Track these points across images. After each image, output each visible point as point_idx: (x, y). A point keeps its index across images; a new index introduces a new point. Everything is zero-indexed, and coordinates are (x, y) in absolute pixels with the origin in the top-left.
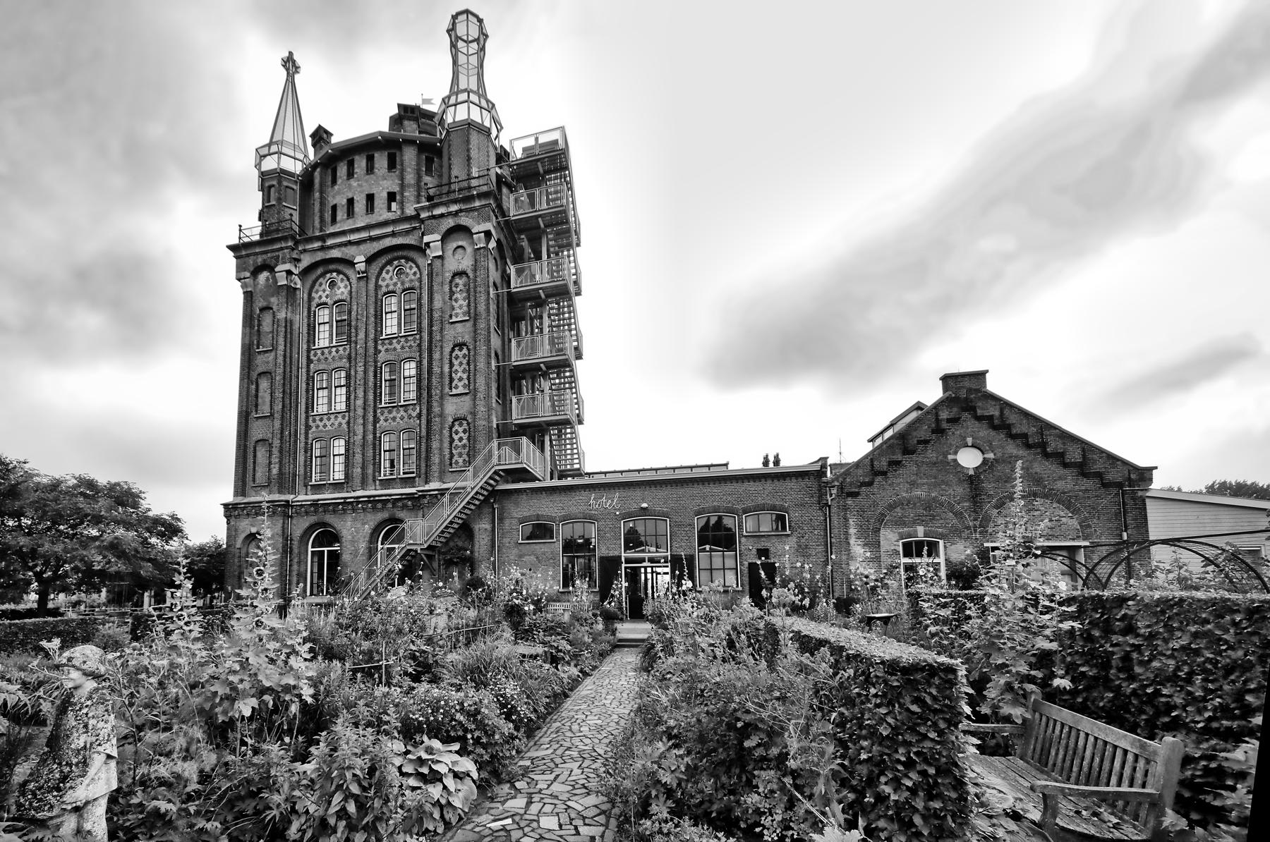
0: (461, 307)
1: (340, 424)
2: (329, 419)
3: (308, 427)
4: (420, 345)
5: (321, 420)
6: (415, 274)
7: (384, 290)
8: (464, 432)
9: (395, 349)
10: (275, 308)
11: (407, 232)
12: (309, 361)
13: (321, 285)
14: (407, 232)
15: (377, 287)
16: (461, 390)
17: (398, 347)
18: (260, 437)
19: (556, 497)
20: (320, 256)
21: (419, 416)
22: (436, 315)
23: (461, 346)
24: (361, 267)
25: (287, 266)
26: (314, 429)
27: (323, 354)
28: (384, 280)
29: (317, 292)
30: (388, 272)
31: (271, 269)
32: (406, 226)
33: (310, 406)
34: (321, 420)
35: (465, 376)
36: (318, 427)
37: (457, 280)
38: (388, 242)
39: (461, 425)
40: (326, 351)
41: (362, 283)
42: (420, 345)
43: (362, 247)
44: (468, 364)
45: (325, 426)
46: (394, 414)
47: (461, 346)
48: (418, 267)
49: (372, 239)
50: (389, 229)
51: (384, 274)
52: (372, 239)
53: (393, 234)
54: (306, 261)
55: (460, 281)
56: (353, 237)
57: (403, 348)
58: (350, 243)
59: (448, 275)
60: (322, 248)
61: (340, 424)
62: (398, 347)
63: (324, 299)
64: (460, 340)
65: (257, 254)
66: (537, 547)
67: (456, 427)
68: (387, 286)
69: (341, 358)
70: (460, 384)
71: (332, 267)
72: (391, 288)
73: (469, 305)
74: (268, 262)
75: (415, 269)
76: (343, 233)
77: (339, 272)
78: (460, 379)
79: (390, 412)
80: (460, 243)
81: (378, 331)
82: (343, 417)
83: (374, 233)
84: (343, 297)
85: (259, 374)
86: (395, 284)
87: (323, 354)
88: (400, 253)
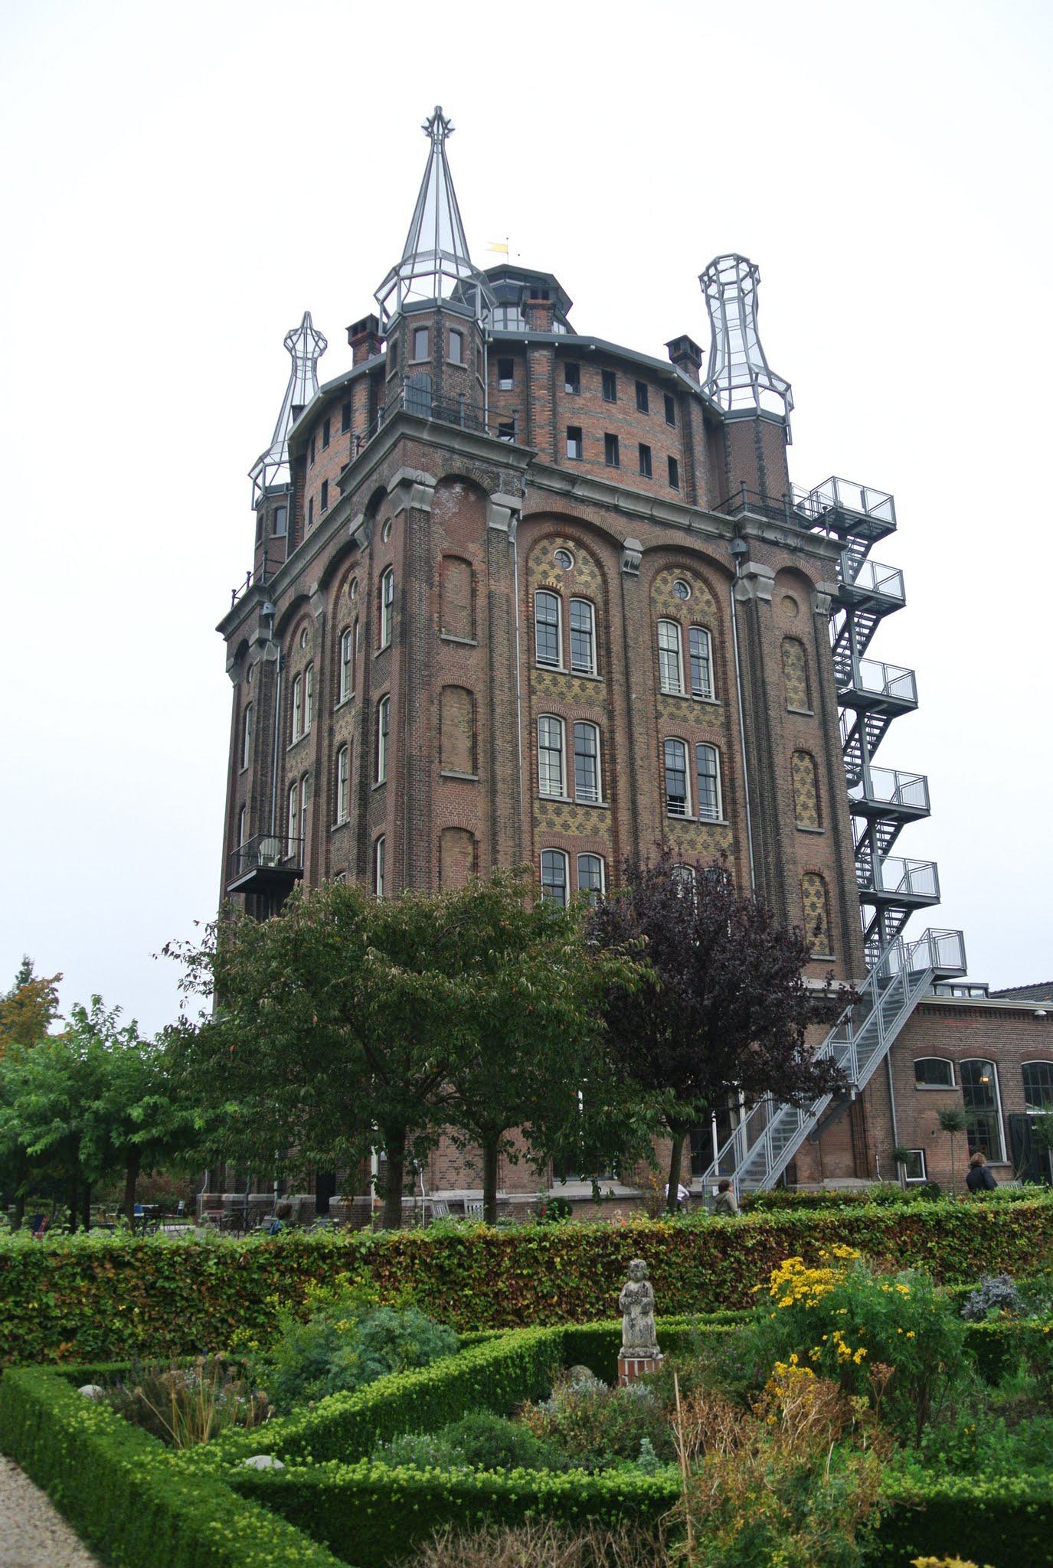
0: (795, 690)
1: (596, 830)
2: (574, 815)
3: (534, 822)
4: (727, 725)
5: (558, 813)
6: (708, 602)
7: (660, 609)
8: (818, 892)
9: (685, 719)
10: (478, 566)
11: (708, 537)
12: (531, 691)
13: (545, 551)
14: (708, 537)
15: (652, 601)
16: (805, 824)
17: (691, 717)
18: (454, 821)
19: (951, 1022)
20: (558, 506)
21: (736, 845)
22: (772, 693)
23: (802, 752)
24: (634, 556)
25: (516, 502)
26: (543, 827)
27: (555, 683)
28: (659, 591)
29: (538, 562)
30: (665, 581)
31: (477, 491)
32: (711, 528)
33: (534, 778)
34: (558, 813)
35: (811, 803)
36: (551, 824)
37: (787, 646)
38: (679, 538)
39: (811, 882)
40: (562, 680)
41: (629, 584)
42: (727, 725)
43: (637, 525)
44: (816, 783)
45: (566, 826)
46: (691, 834)
47: (802, 752)
48: (715, 596)
49: (653, 520)
50: (685, 521)
51: (658, 582)
52: (653, 520)
53: (688, 530)
54: (536, 502)
55: (794, 650)
56: (625, 504)
57: (698, 720)
58: (616, 509)
59: (779, 634)
60: (567, 495)
61: (596, 830)
62: (691, 717)
63: (551, 581)
64: (802, 743)
65: (453, 451)
66: (938, 1096)
67: (806, 885)
68: (665, 604)
69: (590, 703)
70: (806, 814)
71: (570, 530)
72: (672, 611)
73: (808, 690)
74: (475, 476)
75: (708, 596)
76: (613, 490)
77: (580, 544)
78: (805, 807)
79: (685, 830)
80: (791, 593)
81: (657, 680)
82: (602, 819)
83: (661, 514)
84: (589, 592)
85: (444, 687)
86: (678, 607)
87: (555, 683)
88: (688, 561)
